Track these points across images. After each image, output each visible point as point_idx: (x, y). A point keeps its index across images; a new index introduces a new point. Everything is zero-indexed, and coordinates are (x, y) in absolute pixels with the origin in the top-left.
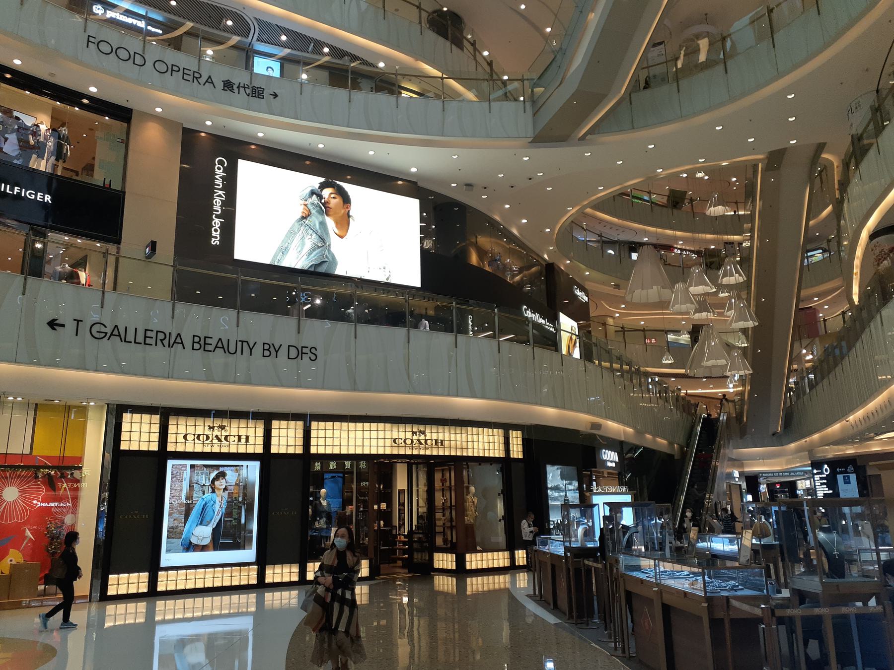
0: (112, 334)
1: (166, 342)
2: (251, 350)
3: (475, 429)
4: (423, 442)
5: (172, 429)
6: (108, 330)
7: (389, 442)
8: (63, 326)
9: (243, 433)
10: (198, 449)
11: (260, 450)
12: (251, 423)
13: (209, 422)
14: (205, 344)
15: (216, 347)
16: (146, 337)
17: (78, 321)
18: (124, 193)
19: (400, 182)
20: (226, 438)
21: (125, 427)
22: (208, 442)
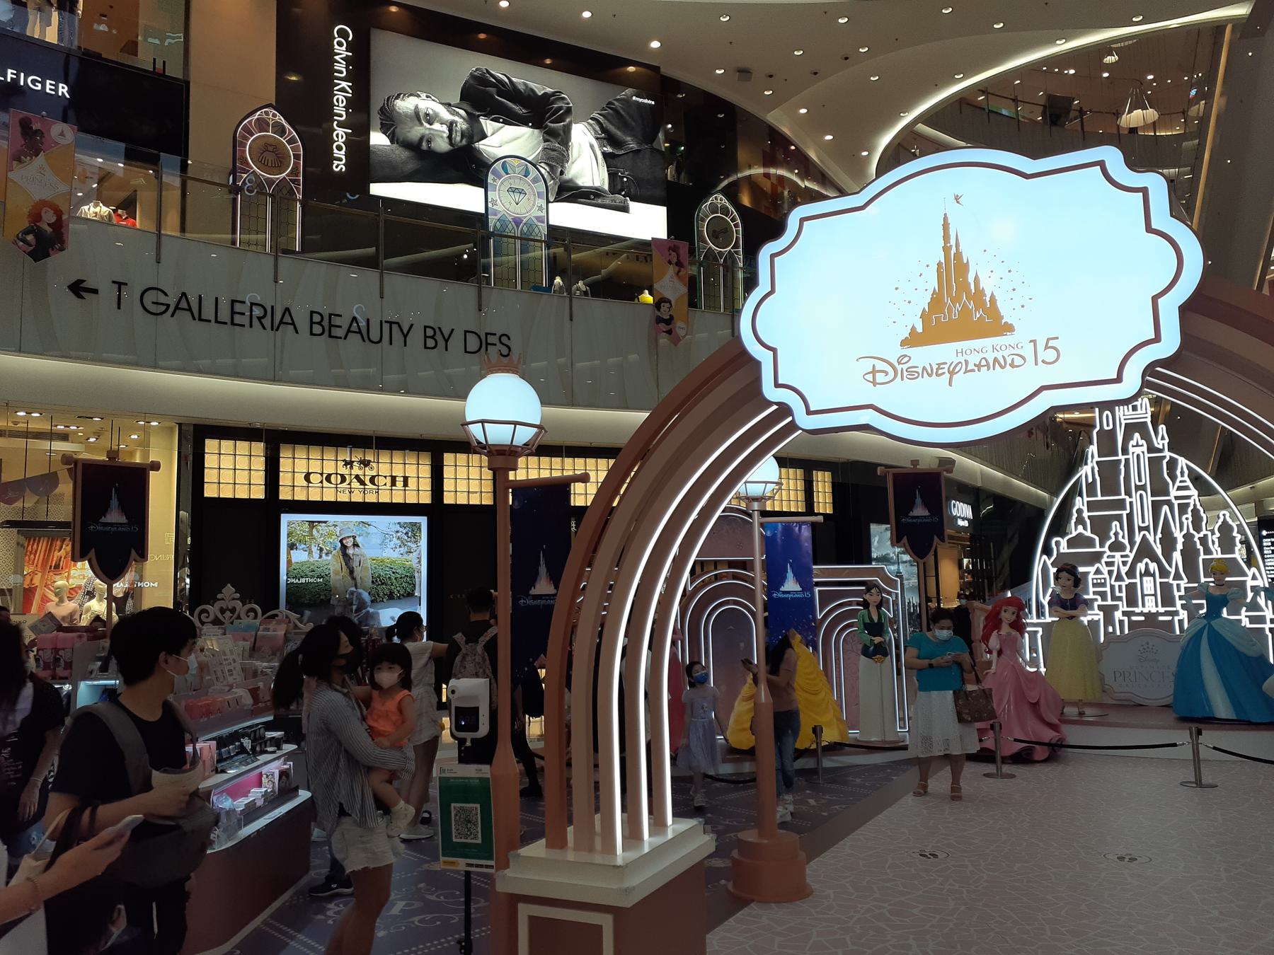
0: (177, 308)
2: (405, 336)
5: (285, 464)
6: (172, 301)
8: (95, 291)
9: (398, 471)
10: (329, 496)
11: (426, 499)
12: (411, 458)
13: (344, 454)
14: (331, 326)
15: (349, 331)
16: (233, 313)
17: (120, 285)
18: (188, 83)
19: (631, 69)
20: (372, 480)
21: (210, 461)
22: (344, 485)
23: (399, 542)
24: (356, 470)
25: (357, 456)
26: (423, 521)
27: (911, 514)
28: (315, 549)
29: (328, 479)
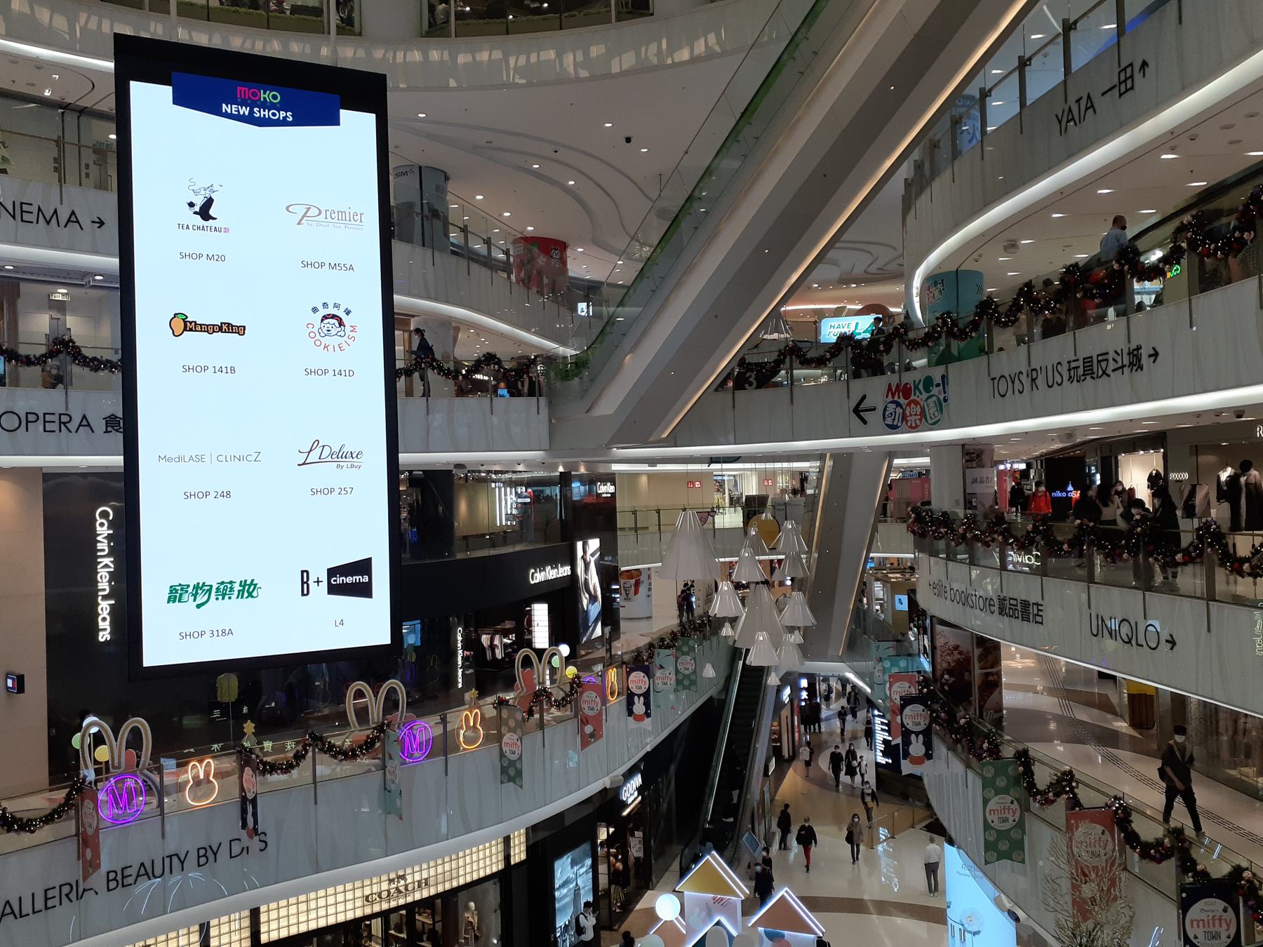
1: (73, 896)
4: (402, 889)
7: (359, 903)
14: (123, 877)
16: (46, 899)
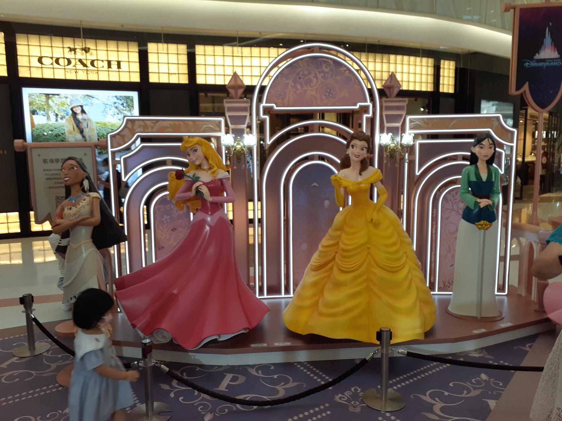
3: (399, 57)
5: (21, 49)
9: (113, 57)
11: (136, 78)
12: (123, 46)
20: (92, 63)
22: (70, 67)
23: (116, 111)
24: (80, 55)
25: (79, 44)
26: (135, 95)
27: (537, 57)
28: (52, 115)
29: (57, 61)
